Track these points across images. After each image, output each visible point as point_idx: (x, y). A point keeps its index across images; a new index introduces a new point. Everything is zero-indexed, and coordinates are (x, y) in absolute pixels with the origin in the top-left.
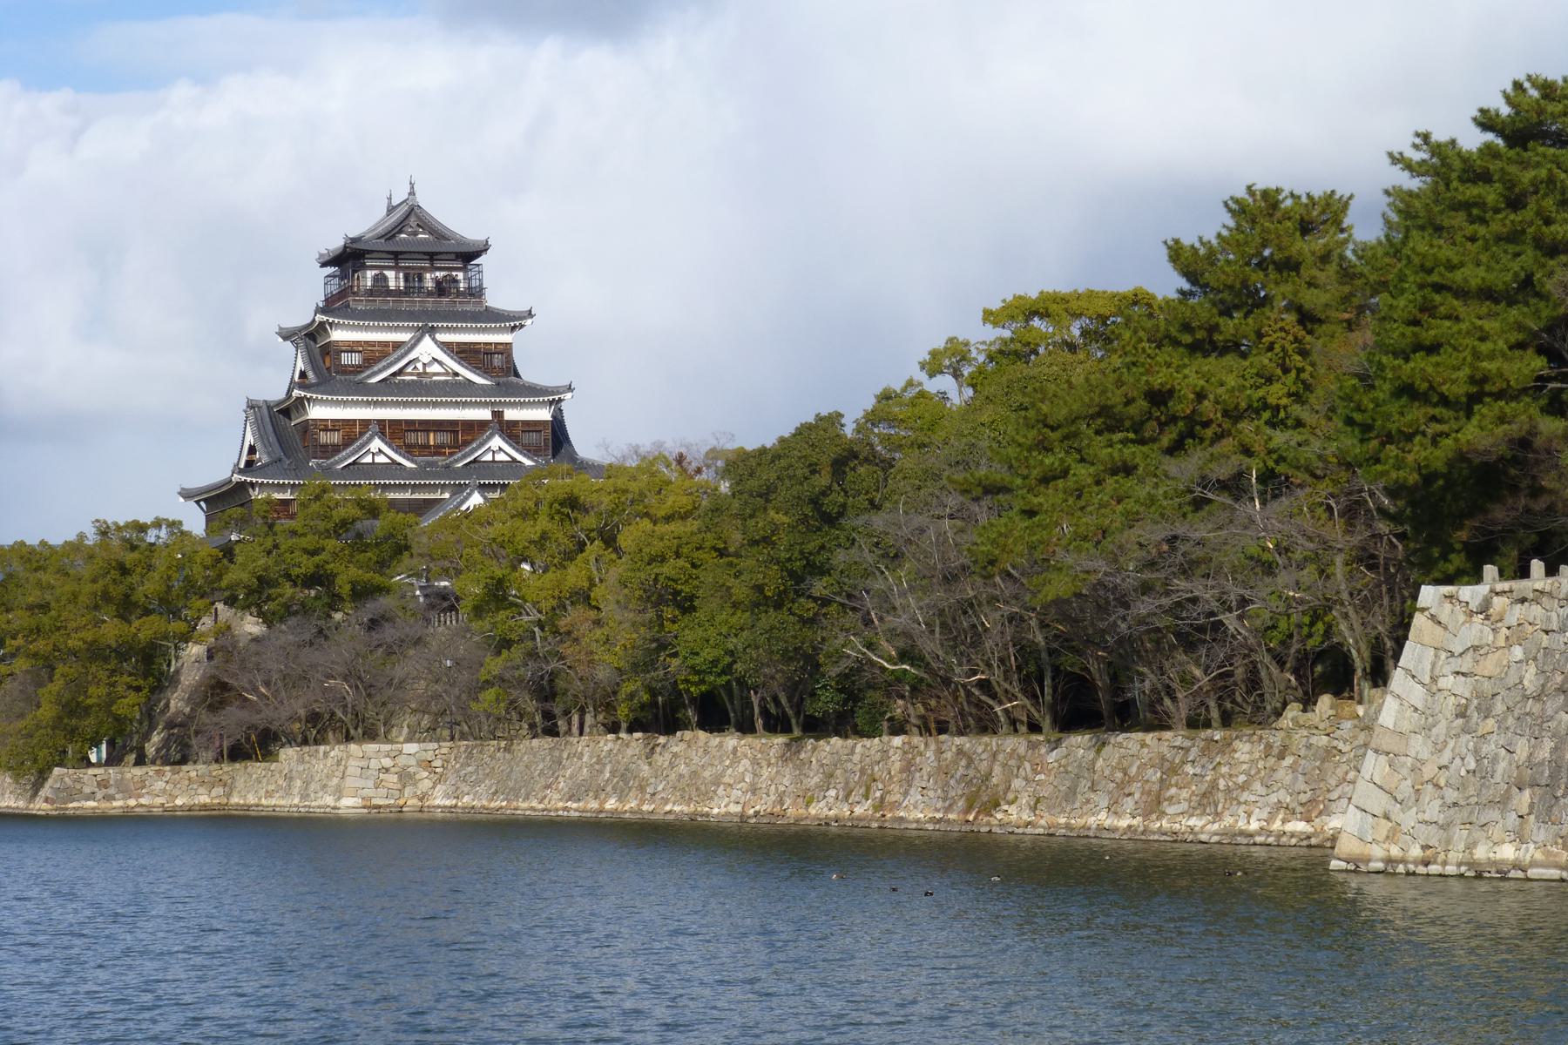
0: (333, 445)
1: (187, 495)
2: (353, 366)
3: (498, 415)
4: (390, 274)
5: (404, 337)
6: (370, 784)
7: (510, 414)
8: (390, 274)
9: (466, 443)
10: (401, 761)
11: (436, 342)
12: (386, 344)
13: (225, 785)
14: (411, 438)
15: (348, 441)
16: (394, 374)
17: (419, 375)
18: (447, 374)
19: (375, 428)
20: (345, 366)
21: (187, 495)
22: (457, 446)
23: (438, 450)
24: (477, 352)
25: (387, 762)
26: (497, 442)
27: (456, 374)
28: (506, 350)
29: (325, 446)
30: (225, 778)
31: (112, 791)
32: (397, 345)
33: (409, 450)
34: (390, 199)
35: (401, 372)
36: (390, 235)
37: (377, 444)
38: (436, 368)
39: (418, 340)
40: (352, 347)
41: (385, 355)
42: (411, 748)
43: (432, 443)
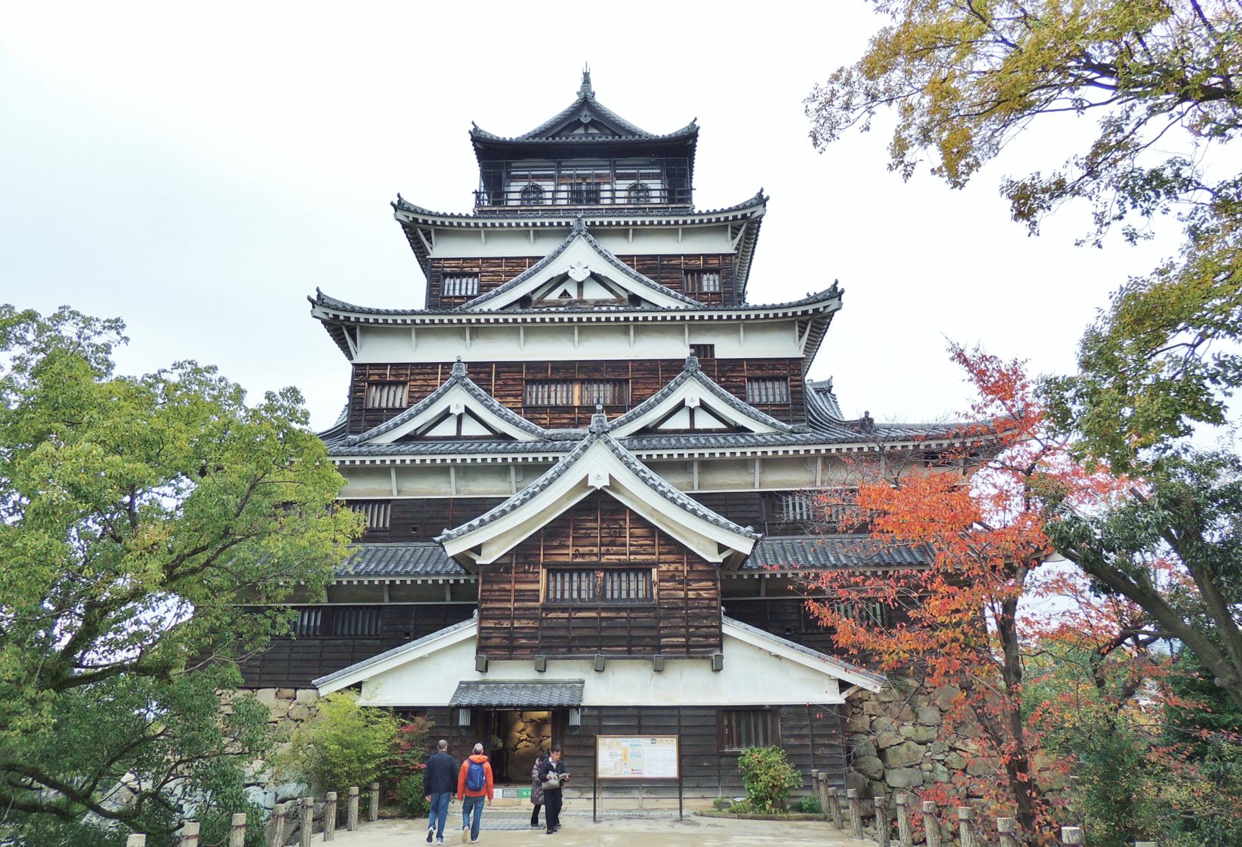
3: (703, 352)
7: (727, 348)
14: (540, 395)
24: (676, 268)
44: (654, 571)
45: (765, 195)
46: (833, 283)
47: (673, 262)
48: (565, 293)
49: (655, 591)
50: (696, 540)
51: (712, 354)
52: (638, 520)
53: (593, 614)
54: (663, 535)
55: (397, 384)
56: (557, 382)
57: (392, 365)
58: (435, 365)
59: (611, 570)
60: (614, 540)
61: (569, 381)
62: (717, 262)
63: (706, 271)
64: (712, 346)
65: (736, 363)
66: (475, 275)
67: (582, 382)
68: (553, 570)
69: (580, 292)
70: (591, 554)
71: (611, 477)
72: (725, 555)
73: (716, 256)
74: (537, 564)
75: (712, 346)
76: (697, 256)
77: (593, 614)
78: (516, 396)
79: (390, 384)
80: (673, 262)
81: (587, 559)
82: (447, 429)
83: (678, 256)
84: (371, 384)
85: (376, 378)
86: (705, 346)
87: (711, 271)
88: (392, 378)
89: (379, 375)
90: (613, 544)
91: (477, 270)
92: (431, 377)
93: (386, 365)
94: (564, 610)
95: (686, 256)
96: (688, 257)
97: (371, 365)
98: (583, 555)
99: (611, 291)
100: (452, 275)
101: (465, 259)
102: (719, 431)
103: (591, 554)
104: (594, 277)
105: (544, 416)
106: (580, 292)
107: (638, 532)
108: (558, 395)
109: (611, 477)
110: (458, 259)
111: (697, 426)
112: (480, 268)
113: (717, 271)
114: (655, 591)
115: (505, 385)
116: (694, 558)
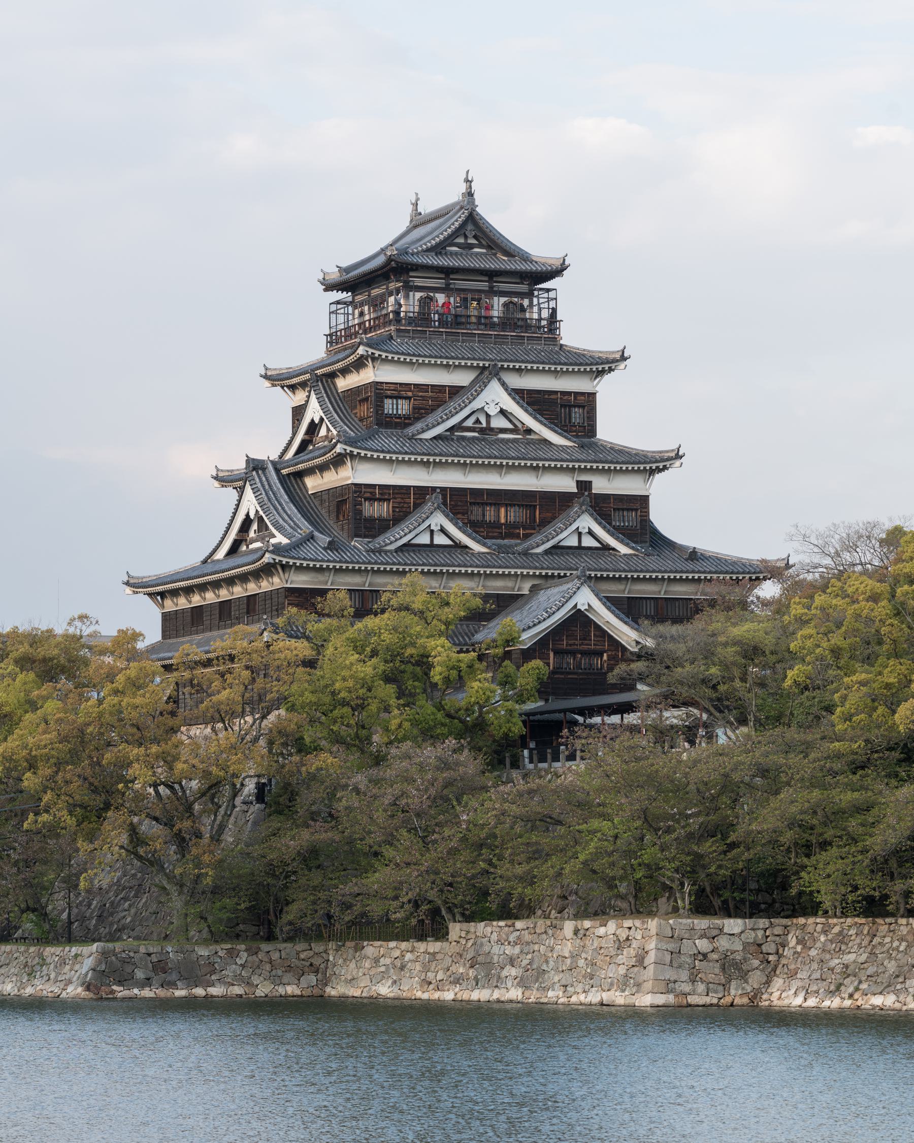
0: (381, 519)
1: (135, 585)
2: (399, 417)
3: (585, 486)
5: (462, 379)
6: (684, 975)
7: (601, 485)
9: (545, 523)
10: (723, 943)
11: (503, 384)
12: (439, 389)
13: (317, 972)
14: (476, 513)
15: (398, 518)
16: (452, 429)
17: (482, 431)
18: (515, 430)
20: (390, 416)
21: (135, 585)
22: (533, 527)
23: (510, 531)
24: (554, 402)
25: (703, 945)
26: (586, 522)
27: (529, 431)
28: (588, 402)
29: (371, 520)
30: (317, 961)
31: (174, 976)
32: (455, 391)
33: (476, 528)
34: (416, 205)
35: (458, 427)
36: (439, 249)
37: (439, 520)
38: (499, 423)
39: (479, 384)
40: (399, 391)
41: (439, 403)
42: (734, 925)
43: (503, 521)
44: (605, 655)
45: (626, 355)
46: (677, 446)
47: (553, 397)
48: (478, 421)
49: (605, 665)
50: (625, 638)
51: (590, 489)
52: (598, 627)
53: (576, 676)
54: (610, 637)
55: (385, 500)
56: (491, 504)
57: (379, 486)
58: (408, 487)
59: (584, 653)
60: (585, 637)
61: (497, 505)
62: (583, 398)
63: (575, 406)
64: (590, 482)
65: (605, 498)
66: (409, 398)
67: (506, 505)
68: (556, 653)
69: (488, 422)
70: (574, 644)
71: (589, 605)
72: (639, 647)
73: (583, 394)
74: (548, 650)
75: (590, 482)
76: (569, 393)
77: (576, 676)
78: (463, 514)
79: (380, 500)
80: (553, 397)
81: (573, 647)
82: (425, 539)
83: (556, 392)
84: (366, 499)
85: (368, 495)
86: (586, 482)
87: (579, 407)
88: (380, 497)
89: (371, 493)
90: (585, 639)
91: (410, 394)
92: (406, 496)
93: (375, 486)
94: (562, 673)
95: (562, 393)
96: (564, 393)
97: (365, 485)
98: (571, 645)
99: (510, 421)
101: (401, 384)
102: (596, 548)
103: (574, 644)
104: (502, 412)
105: (482, 530)
106: (488, 422)
107: (597, 633)
108: (490, 514)
109: (589, 605)
110: (396, 384)
111: (583, 544)
113: (583, 407)
114: (605, 665)
115: (456, 505)
116: (624, 649)
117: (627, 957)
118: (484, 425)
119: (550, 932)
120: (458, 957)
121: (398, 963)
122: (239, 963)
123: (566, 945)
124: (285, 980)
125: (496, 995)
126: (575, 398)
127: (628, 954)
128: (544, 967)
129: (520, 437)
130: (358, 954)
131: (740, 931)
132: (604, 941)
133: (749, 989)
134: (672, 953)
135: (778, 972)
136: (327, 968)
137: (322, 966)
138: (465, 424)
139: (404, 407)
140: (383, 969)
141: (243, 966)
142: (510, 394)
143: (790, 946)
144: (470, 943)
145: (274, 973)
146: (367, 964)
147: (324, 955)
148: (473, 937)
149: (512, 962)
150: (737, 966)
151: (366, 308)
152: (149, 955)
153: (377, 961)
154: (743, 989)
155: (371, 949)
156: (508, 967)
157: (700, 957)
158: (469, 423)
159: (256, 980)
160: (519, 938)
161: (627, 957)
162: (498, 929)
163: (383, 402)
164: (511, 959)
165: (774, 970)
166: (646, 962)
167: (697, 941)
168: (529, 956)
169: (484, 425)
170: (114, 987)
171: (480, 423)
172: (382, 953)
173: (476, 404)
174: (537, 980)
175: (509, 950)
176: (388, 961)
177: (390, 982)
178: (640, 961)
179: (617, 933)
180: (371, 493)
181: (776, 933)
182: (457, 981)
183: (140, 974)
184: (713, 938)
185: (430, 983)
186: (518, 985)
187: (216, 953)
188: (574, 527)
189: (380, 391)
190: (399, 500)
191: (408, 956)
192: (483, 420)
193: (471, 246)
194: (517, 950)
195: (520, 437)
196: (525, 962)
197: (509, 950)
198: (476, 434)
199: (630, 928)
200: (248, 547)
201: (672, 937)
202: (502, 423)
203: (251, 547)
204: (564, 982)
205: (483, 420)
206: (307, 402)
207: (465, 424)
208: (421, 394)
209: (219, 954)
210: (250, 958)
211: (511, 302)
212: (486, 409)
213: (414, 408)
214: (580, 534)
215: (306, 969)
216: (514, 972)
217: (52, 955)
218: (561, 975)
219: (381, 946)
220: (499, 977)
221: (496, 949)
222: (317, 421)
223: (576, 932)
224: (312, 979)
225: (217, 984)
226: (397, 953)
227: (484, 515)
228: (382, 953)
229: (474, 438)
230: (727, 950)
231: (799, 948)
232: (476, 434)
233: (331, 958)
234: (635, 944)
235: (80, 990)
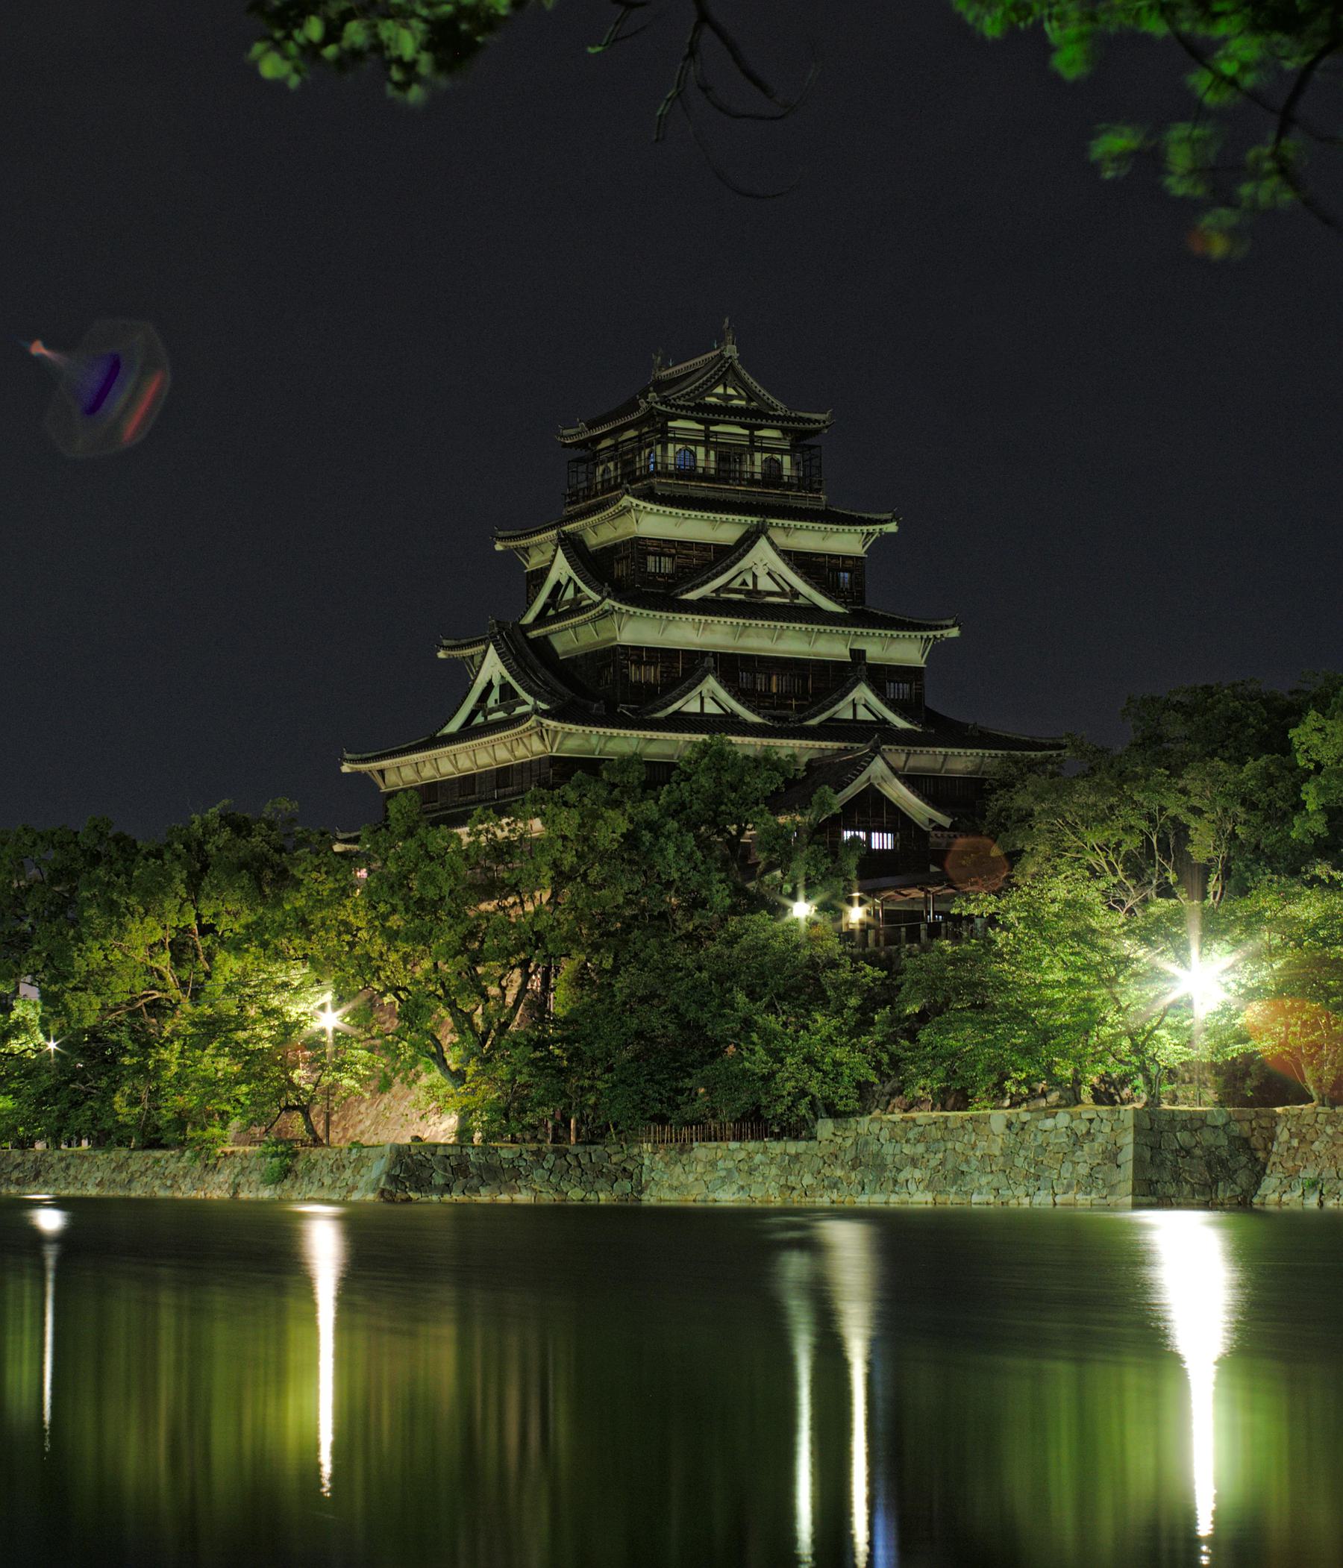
2: (663, 575)
4: (701, 452)
8: (701, 452)
11: (772, 544)
12: (704, 547)
13: (631, 1177)
16: (716, 591)
17: (748, 593)
18: (782, 594)
19: (710, 662)
20: (654, 574)
26: (863, 693)
27: (796, 594)
35: (725, 588)
37: (711, 684)
39: (747, 542)
43: (774, 690)
48: (744, 583)
62: (851, 562)
73: (851, 558)
80: (819, 560)
85: (635, 657)
91: (673, 551)
99: (778, 584)
100: (654, 554)
102: (872, 722)
106: (755, 584)
112: (674, 548)
117: (1088, 1155)
118: (751, 587)
119: (970, 1127)
120: (833, 1158)
121: (744, 1167)
122: (546, 1167)
123: (994, 1141)
124: (597, 1186)
125: (894, 1199)
126: (843, 562)
127: (1091, 1149)
128: (964, 1168)
129: (787, 601)
130: (685, 1156)
131: (1224, 1121)
132: (1052, 1135)
133: (1238, 1190)
134: (1152, 1148)
135: (1268, 1171)
136: (641, 1173)
137: (636, 1171)
138: (731, 586)
139: (667, 565)
140: (723, 1173)
141: (551, 1171)
142: (779, 555)
143: (1282, 1140)
144: (849, 1142)
145: (584, 1179)
146: (700, 1169)
147: (638, 1158)
148: (854, 1134)
149: (914, 1162)
150: (1222, 1162)
151: (611, 465)
152: (448, 1157)
153: (713, 1164)
154: (1232, 1190)
155: (702, 1151)
156: (908, 1169)
157: (1183, 1153)
158: (736, 584)
159: (564, 1186)
160: (922, 1134)
161: (1088, 1155)
162: (890, 1125)
163: (646, 559)
164: (913, 1159)
165: (1264, 1169)
166: (1121, 1159)
167: (1178, 1134)
168: (940, 1155)
169: (751, 587)
170: (411, 1194)
171: (747, 585)
172: (719, 1154)
173: (744, 563)
174: (954, 1183)
175: (907, 1149)
176: (730, 1164)
177: (735, 1188)
178: (1112, 1156)
179: (1073, 1125)
180: (638, 656)
181: (1264, 1125)
182: (834, 1185)
183: (438, 1179)
184: (1196, 1130)
185: (794, 1189)
186: (927, 1187)
187: (521, 1155)
188: (850, 697)
189: (639, 547)
190: (667, 664)
191: (758, 1158)
192: (750, 582)
193: (732, 397)
194: (921, 1148)
195: (787, 601)
196: (933, 1163)
197: (907, 1149)
198: (742, 597)
199: (1091, 1121)
200: (486, 718)
201: (1151, 1129)
202: (772, 587)
203: (490, 718)
204: (995, 1184)
205: (750, 582)
206: (552, 561)
207: (731, 586)
208: (685, 552)
209: (524, 1156)
210: (558, 1162)
211: (772, 459)
212: (754, 569)
213: (678, 567)
214: (855, 706)
215: (619, 1174)
216: (918, 1174)
217: (323, 1158)
218: (990, 1177)
219: (718, 1147)
220: (895, 1182)
221: (888, 1149)
222: (564, 582)
223: (1009, 1125)
224: (627, 1185)
225: (524, 1191)
226: (742, 1155)
227: (755, 683)
228: (719, 1154)
229: (740, 601)
230: (1212, 1146)
231: (1295, 1143)
232: (742, 597)
233: (647, 1162)
234: (1100, 1139)
235: (371, 1197)
